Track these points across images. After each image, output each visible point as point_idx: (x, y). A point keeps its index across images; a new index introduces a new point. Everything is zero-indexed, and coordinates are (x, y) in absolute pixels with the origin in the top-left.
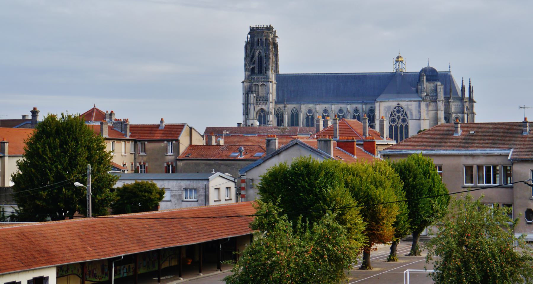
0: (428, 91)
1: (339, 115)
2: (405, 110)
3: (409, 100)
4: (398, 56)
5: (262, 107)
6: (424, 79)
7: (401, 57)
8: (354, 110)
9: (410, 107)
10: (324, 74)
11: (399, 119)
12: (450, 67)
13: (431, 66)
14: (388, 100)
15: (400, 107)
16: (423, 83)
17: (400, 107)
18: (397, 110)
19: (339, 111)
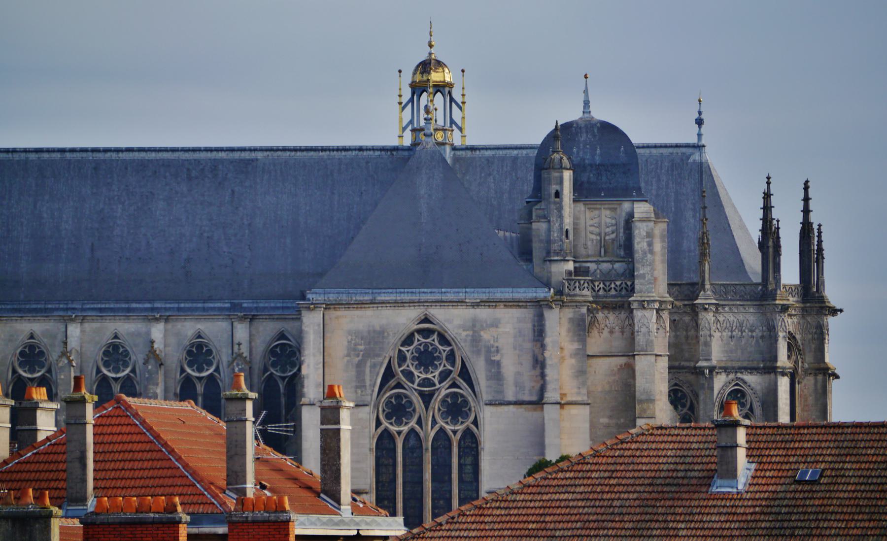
0: (582, 251)
1: (105, 377)
2: (464, 349)
3: (484, 297)
4: (423, 57)
6: (561, 182)
7: (439, 64)
8: (189, 353)
9: (486, 335)
10: (26, 151)
11: (427, 398)
12: (699, 122)
13: (599, 114)
14: (367, 298)
15: (435, 336)
16: (560, 209)
17: (435, 336)
18: (417, 350)
19: (106, 353)
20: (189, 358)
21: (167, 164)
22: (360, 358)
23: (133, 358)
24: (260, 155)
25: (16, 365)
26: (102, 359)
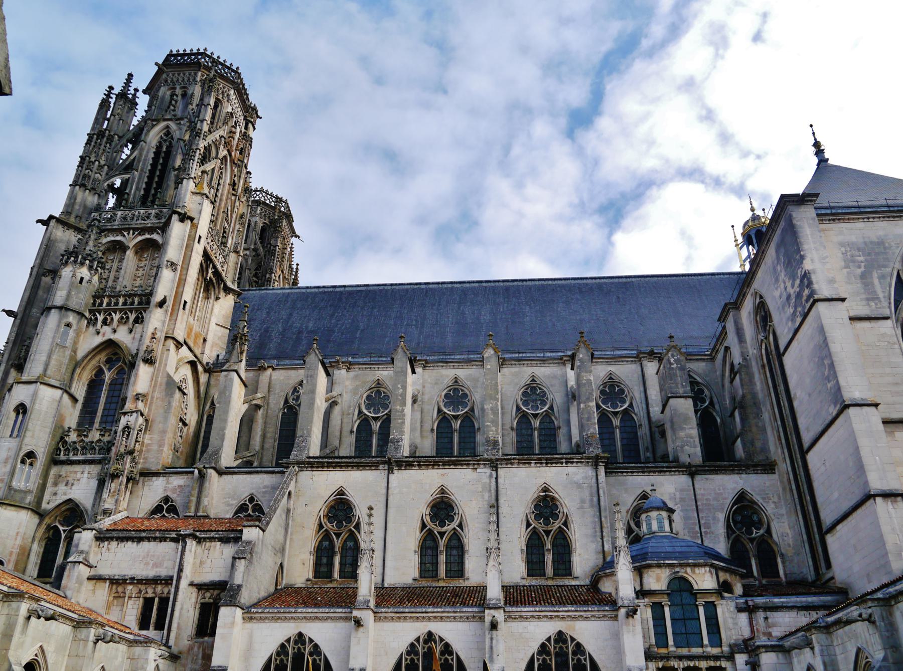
19: (525, 394)
20: (603, 397)
21: (563, 286)
22: (863, 269)
23: (550, 397)
24: (634, 280)
26: (521, 399)
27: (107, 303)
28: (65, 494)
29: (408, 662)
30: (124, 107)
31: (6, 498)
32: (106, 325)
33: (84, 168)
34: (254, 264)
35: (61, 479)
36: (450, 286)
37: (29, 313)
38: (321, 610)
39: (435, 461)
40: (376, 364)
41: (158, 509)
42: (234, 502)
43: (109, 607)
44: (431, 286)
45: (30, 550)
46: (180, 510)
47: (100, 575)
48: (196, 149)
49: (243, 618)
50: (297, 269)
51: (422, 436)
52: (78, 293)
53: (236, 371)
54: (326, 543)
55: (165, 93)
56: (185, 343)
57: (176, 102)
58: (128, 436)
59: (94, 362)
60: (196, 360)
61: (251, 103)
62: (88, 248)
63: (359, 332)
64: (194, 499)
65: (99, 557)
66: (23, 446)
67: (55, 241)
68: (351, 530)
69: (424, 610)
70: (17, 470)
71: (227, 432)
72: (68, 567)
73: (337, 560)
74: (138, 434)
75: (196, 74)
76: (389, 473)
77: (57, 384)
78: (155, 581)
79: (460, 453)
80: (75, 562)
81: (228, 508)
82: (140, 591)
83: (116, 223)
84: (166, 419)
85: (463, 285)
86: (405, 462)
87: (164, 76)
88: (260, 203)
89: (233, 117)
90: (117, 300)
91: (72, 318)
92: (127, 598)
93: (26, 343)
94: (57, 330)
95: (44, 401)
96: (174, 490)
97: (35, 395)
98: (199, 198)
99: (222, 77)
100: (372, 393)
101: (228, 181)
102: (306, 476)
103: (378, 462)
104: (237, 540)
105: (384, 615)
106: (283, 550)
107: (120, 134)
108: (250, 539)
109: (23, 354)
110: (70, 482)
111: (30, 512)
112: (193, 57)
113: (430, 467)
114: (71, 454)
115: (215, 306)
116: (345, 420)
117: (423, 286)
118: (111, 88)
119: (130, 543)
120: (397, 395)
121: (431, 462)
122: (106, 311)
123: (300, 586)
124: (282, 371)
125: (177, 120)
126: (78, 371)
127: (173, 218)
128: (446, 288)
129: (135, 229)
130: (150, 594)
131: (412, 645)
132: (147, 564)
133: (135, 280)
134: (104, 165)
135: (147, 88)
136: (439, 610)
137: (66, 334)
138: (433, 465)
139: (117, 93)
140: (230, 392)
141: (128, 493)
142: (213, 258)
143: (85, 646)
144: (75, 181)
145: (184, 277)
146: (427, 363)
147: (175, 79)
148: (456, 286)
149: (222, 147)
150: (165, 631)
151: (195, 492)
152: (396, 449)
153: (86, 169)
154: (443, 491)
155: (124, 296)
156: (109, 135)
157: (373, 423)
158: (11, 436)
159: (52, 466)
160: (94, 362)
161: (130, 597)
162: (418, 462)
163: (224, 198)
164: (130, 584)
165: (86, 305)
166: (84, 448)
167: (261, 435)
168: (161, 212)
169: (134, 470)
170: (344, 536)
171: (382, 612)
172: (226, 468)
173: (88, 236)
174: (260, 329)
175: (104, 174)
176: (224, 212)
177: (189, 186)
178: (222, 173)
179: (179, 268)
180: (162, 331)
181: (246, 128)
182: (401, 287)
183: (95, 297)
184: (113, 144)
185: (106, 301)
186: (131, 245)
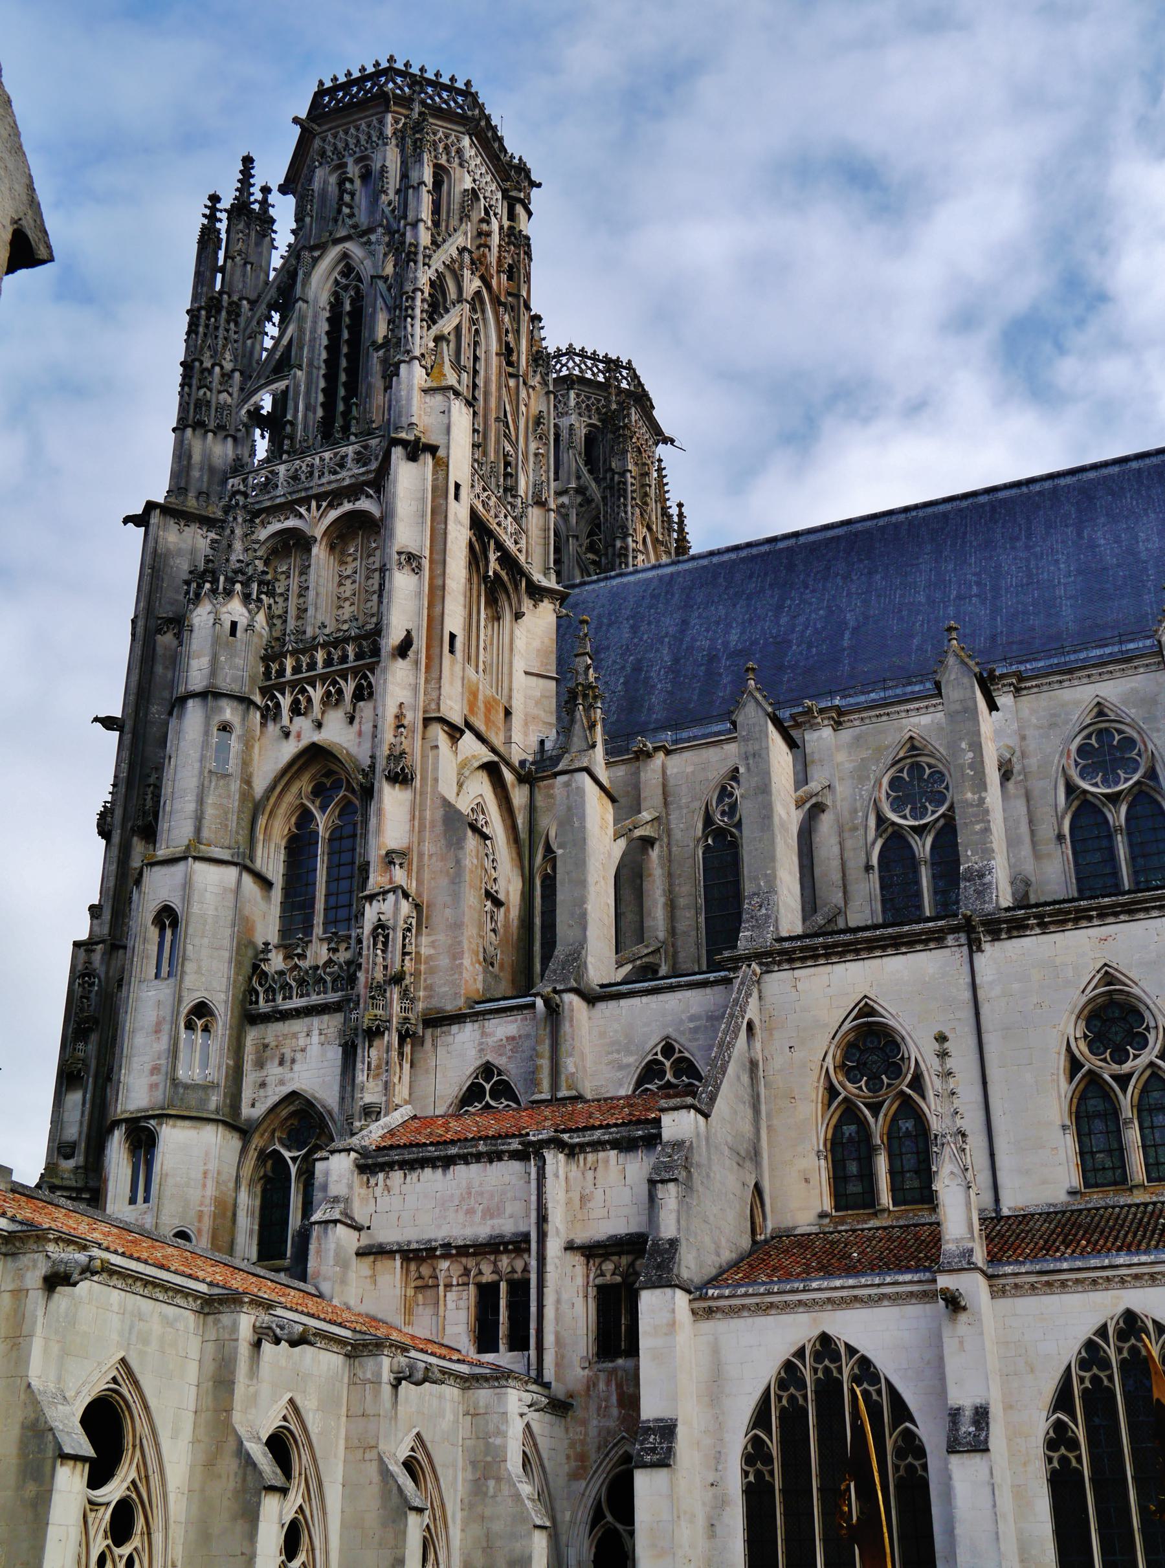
5: (317, 737)
25: (1074, 774)
27: (293, 668)
28: (282, 1082)
29: (1088, 1384)
30: (248, 235)
31: (171, 1105)
32: (299, 714)
33: (194, 388)
34: (583, 523)
35: (268, 1053)
36: (1048, 485)
37: (146, 715)
38: (863, 1281)
39: (1078, 910)
40: (900, 702)
41: (472, 1094)
42: (631, 1059)
43: (408, 1311)
44: (1001, 495)
45: (235, 1206)
46: (518, 1088)
47: (380, 1245)
48: (414, 291)
49: (694, 1312)
50: (681, 515)
51: (1037, 856)
52: (232, 656)
53: (588, 770)
54: (850, 1130)
55: (326, 182)
56: (468, 725)
57: (352, 194)
58: (385, 944)
59: (290, 798)
60: (496, 759)
61: (512, 157)
62: (233, 558)
63: (847, 636)
64: (545, 1063)
65: (372, 1208)
66: (185, 993)
67: (168, 554)
68: (902, 1093)
69: (1106, 1262)
70: (182, 1045)
71: (589, 907)
72: (315, 1234)
73: (882, 1164)
74: (404, 938)
75: (381, 122)
76: (971, 952)
77: (225, 855)
78: (492, 1247)
79: (1137, 883)
80: (327, 1222)
81: (619, 1074)
82: (466, 1272)
83: (280, 491)
84: (456, 897)
85: (1080, 476)
86: (1005, 922)
87: (317, 143)
88: (573, 382)
89: (478, 199)
90: (312, 657)
91: (229, 712)
92: (441, 1288)
93: (152, 780)
94: (205, 744)
95: (208, 895)
96: (499, 1048)
97: (187, 885)
98: (439, 398)
99: (438, 112)
100: (901, 771)
101: (494, 347)
102: (779, 982)
103: (941, 930)
104: (652, 1140)
105: (1011, 1281)
106: (755, 1155)
107: (253, 296)
108: (679, 1137)
109: (149, 803)
110: (288, 1057)
111: (221, 1128)
112: (369, 84)
113: (1070, 925)
114: (279, 998)
115: (517, 633)
116: (849, 844)
117: (983, 499)
118: (214, 198)
119: (428, 1171)
120: (962, 767)
121: (1069, 912)
122: (293, 684)
123: (808, 1230)
124: (687, 755)
125: (361, 234)
126: (262, 821)
127: (393, 457)
128: (1040, 493)
129: (319, 497)
130: (488, 1277)
131: (1090, 1345)
132: (470, 1212)
133: (341, 607)
134: (233, 371)
135: (288, 179)
136: (1144, 1258)
137: (223, 748)
138: (1076, 920)
139: (228, 207)
140: (582, 818)
141: (406, 1066)
142: (494, 526)
143: (377, 1394)
144: (181, 420)
145: (440, 582)
146: (1021, 679)
147: (340, 145)
148: (1062, 482)
149: (467, 273)
150: (533, 1352)
151: (545, 1048)
152: (980, 894)
153: (199, 388)
154: (1108, 977)
155: (324, 645)
156: (231, 304)
157: (915, 841)
158: (157, 976)
159: (248, 1028)
160: (290, 798)
161: (448, 1286)
162: (1035, 917)
163: (493, 387)
164: (444, 1256)
165: (252, 679)
166: (301, 982)
167: (665, 904)
168: (366, 447)
169: (410, 1015)
170: (889, 1108)
171: (1005, 1275)
172: (602, 986)
173: (228, 531)
174: (623, 668)
175: (235, 390)
176: (497, 419)
177: (415, 376)
178: (477, 331)
179: (426, 563)
180: (414, 709)
181: (512, 216)
182: (930, 510)
183: (266, 659)
184: (242, 320)
185: (289, 663)
186: (318, 532)
